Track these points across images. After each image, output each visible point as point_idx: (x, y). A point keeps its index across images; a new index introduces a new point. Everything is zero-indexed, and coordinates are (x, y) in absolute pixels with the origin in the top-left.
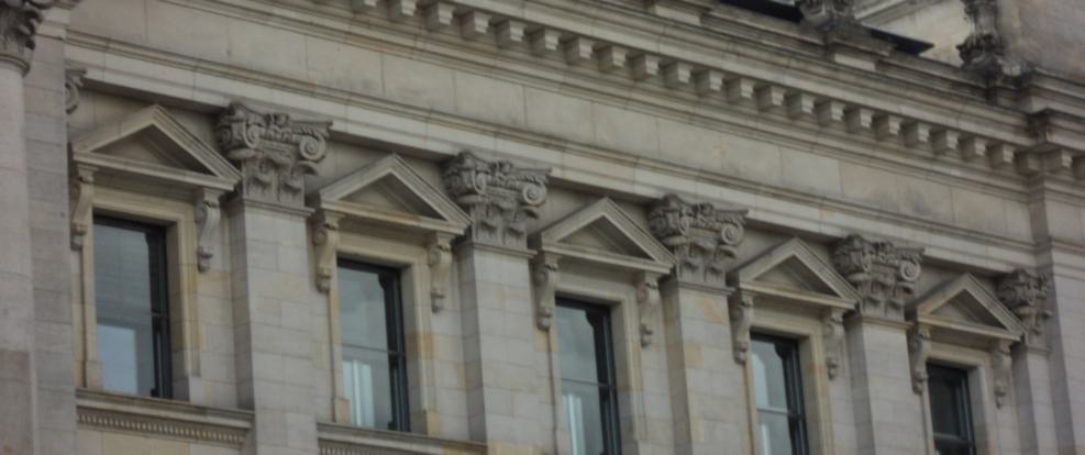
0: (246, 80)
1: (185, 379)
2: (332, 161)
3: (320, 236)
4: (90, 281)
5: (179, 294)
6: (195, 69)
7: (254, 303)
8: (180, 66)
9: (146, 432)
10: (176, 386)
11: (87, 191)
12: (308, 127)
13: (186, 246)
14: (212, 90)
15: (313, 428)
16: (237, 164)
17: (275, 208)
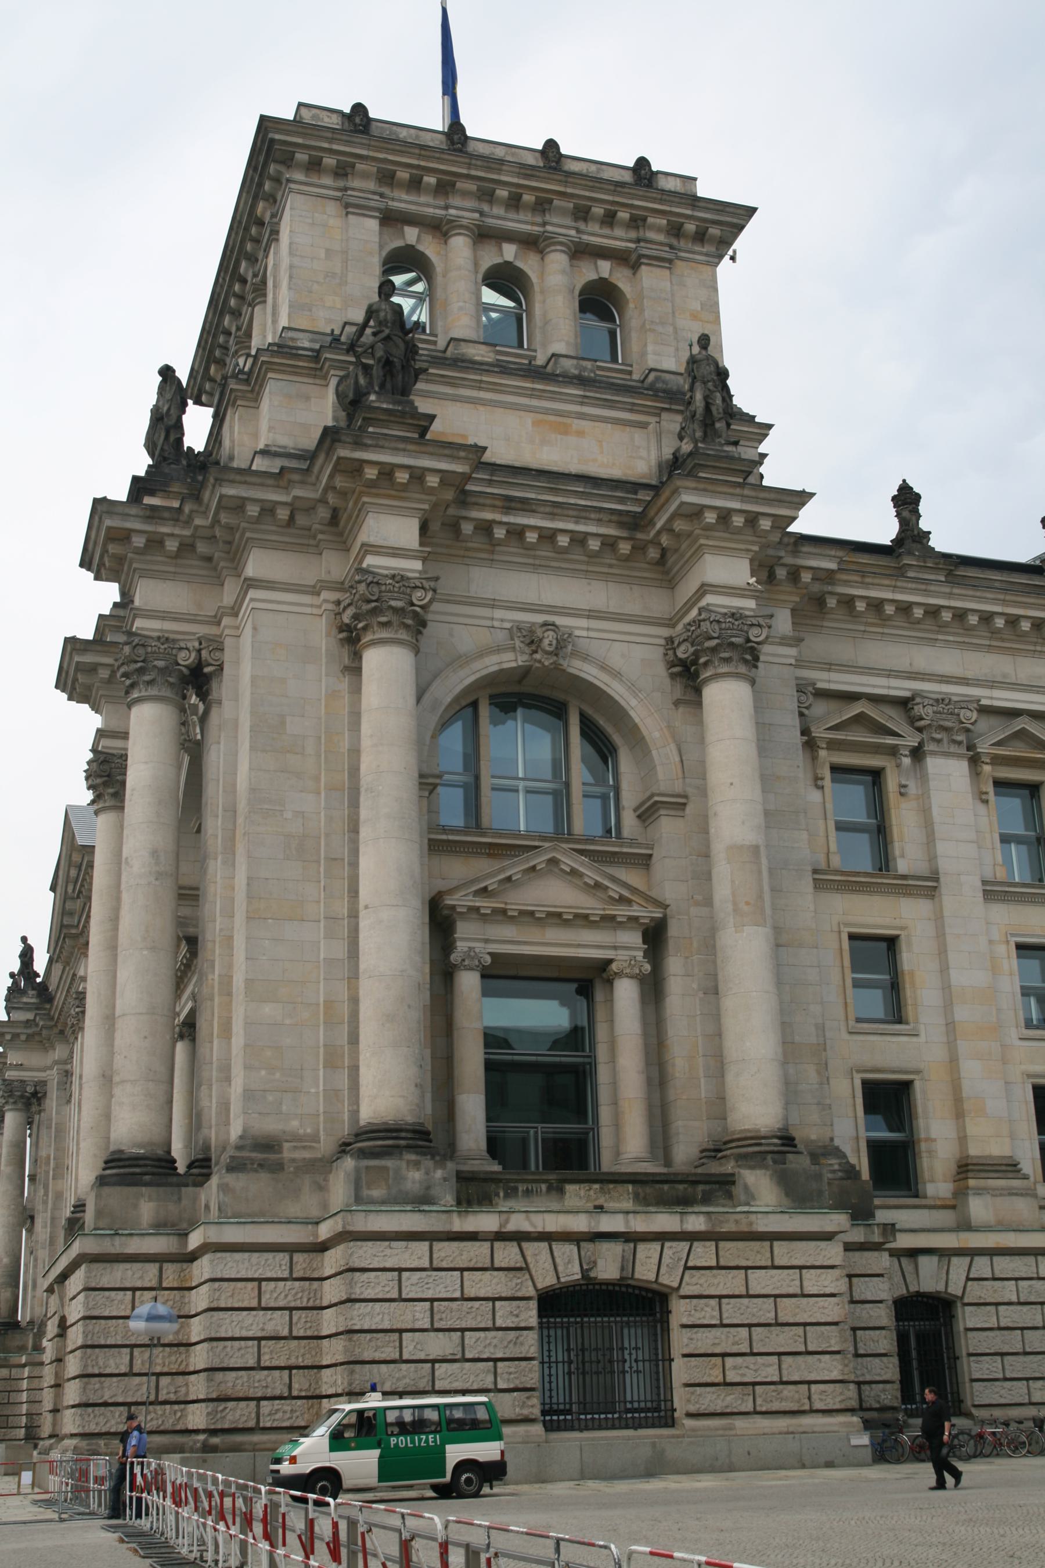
0: (923, 680)
1: (895, 859)
2: (984, 724)
3: (979, 769)
4: (829, 806)
5: (889, 810)
6: (889, 676)
7: (935, 811)
8: (878, 675)
9: (870, 893)
10: (891, 864)
11: (823, 753)
12: (965, 703)
13: (891, 782)
14: (900, 688)
15: (980, 884)
16: (920, 730)
17: (947, 754)
